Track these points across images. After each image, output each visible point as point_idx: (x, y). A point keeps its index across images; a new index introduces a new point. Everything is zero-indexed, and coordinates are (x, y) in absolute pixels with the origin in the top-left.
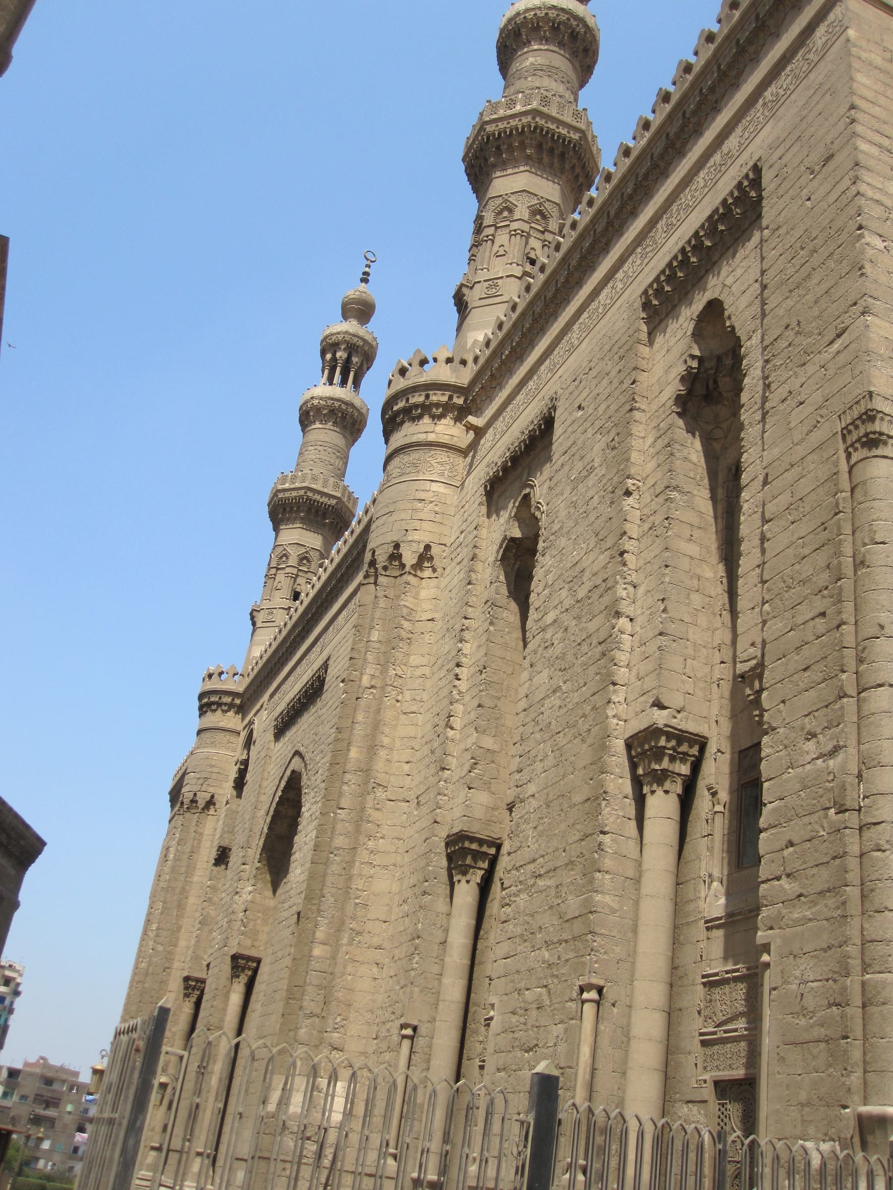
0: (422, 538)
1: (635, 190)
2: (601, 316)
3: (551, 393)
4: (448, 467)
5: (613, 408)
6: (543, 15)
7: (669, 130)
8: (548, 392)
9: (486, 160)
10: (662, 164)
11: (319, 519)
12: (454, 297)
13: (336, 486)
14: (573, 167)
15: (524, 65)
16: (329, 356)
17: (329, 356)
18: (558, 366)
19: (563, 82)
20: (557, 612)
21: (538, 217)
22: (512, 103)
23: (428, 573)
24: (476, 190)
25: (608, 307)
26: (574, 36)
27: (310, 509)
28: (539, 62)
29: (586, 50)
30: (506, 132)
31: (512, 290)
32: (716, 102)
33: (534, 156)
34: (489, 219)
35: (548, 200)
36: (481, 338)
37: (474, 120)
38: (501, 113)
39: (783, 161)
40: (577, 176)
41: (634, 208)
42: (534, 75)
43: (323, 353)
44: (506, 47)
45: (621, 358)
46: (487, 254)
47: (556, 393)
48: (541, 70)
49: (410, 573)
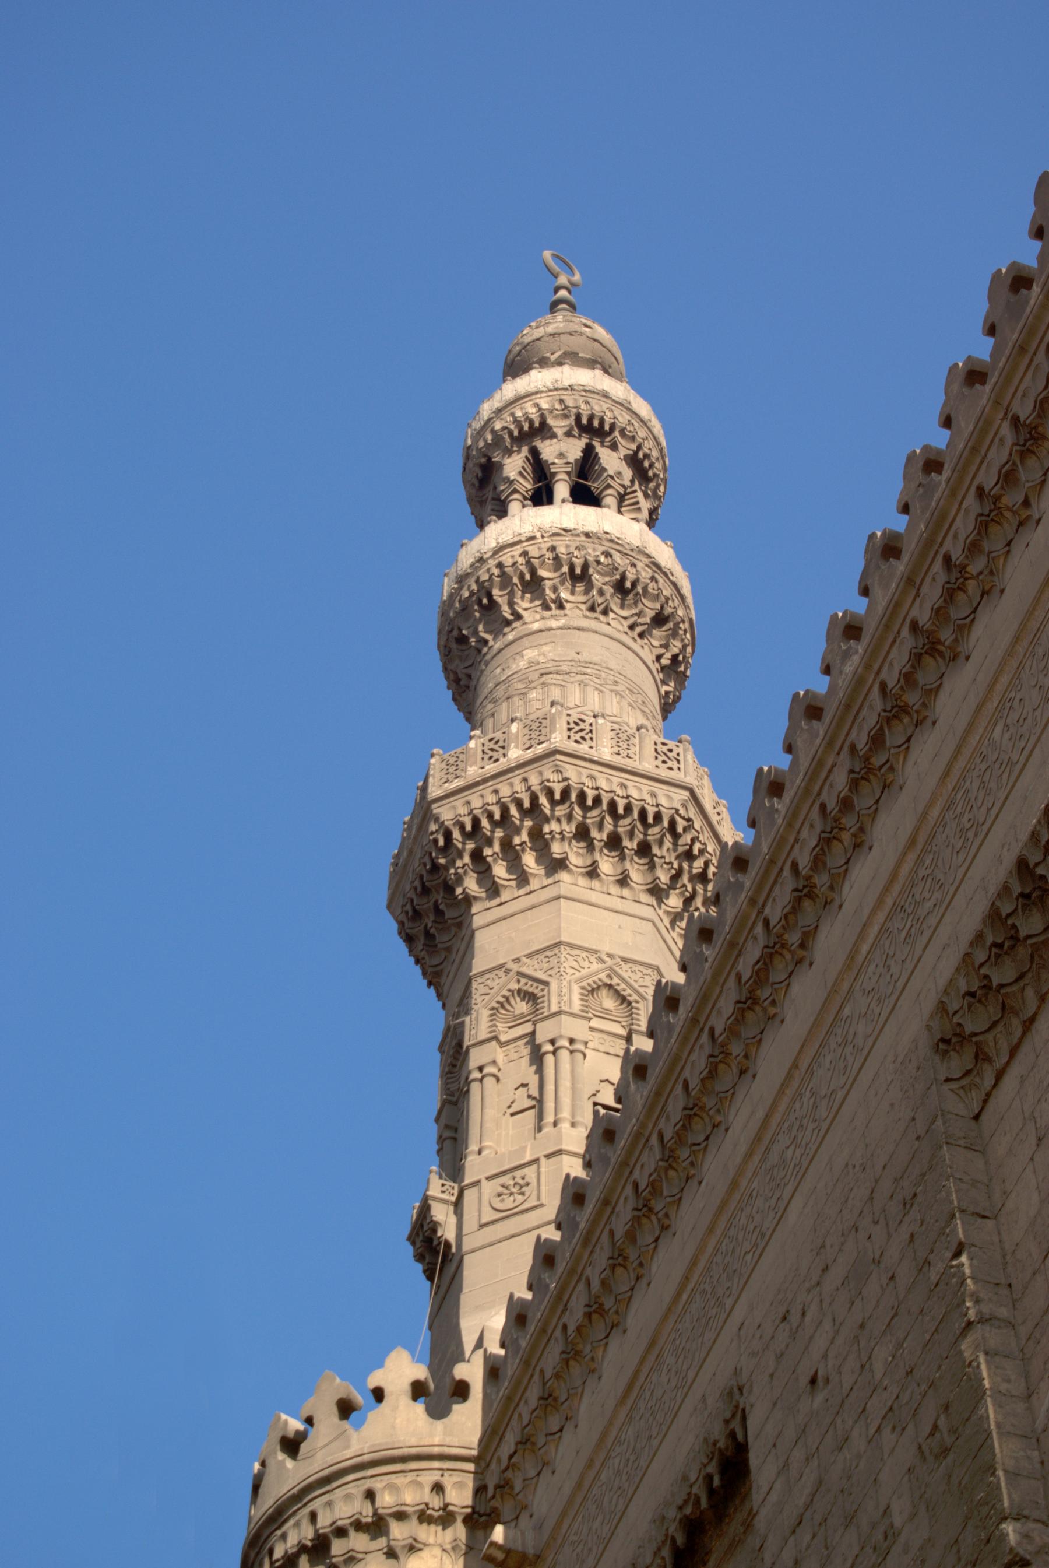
1: (854, 784)
2: (824, 1126)
7: (914, 613)
10: (912, 698)
12: (412, 1239)
15: (514, 668)
18: (729, 1302)
19: (617, 693)
21: (609, 1003)
24: (434, 978)
25: (840, 1095)
28: (551, 655)
32: (1026, 503)
35: (626, 960)
36: (497, 1320)
41: (862, 829)
45: (907, 1204)
47: (736, 1372)
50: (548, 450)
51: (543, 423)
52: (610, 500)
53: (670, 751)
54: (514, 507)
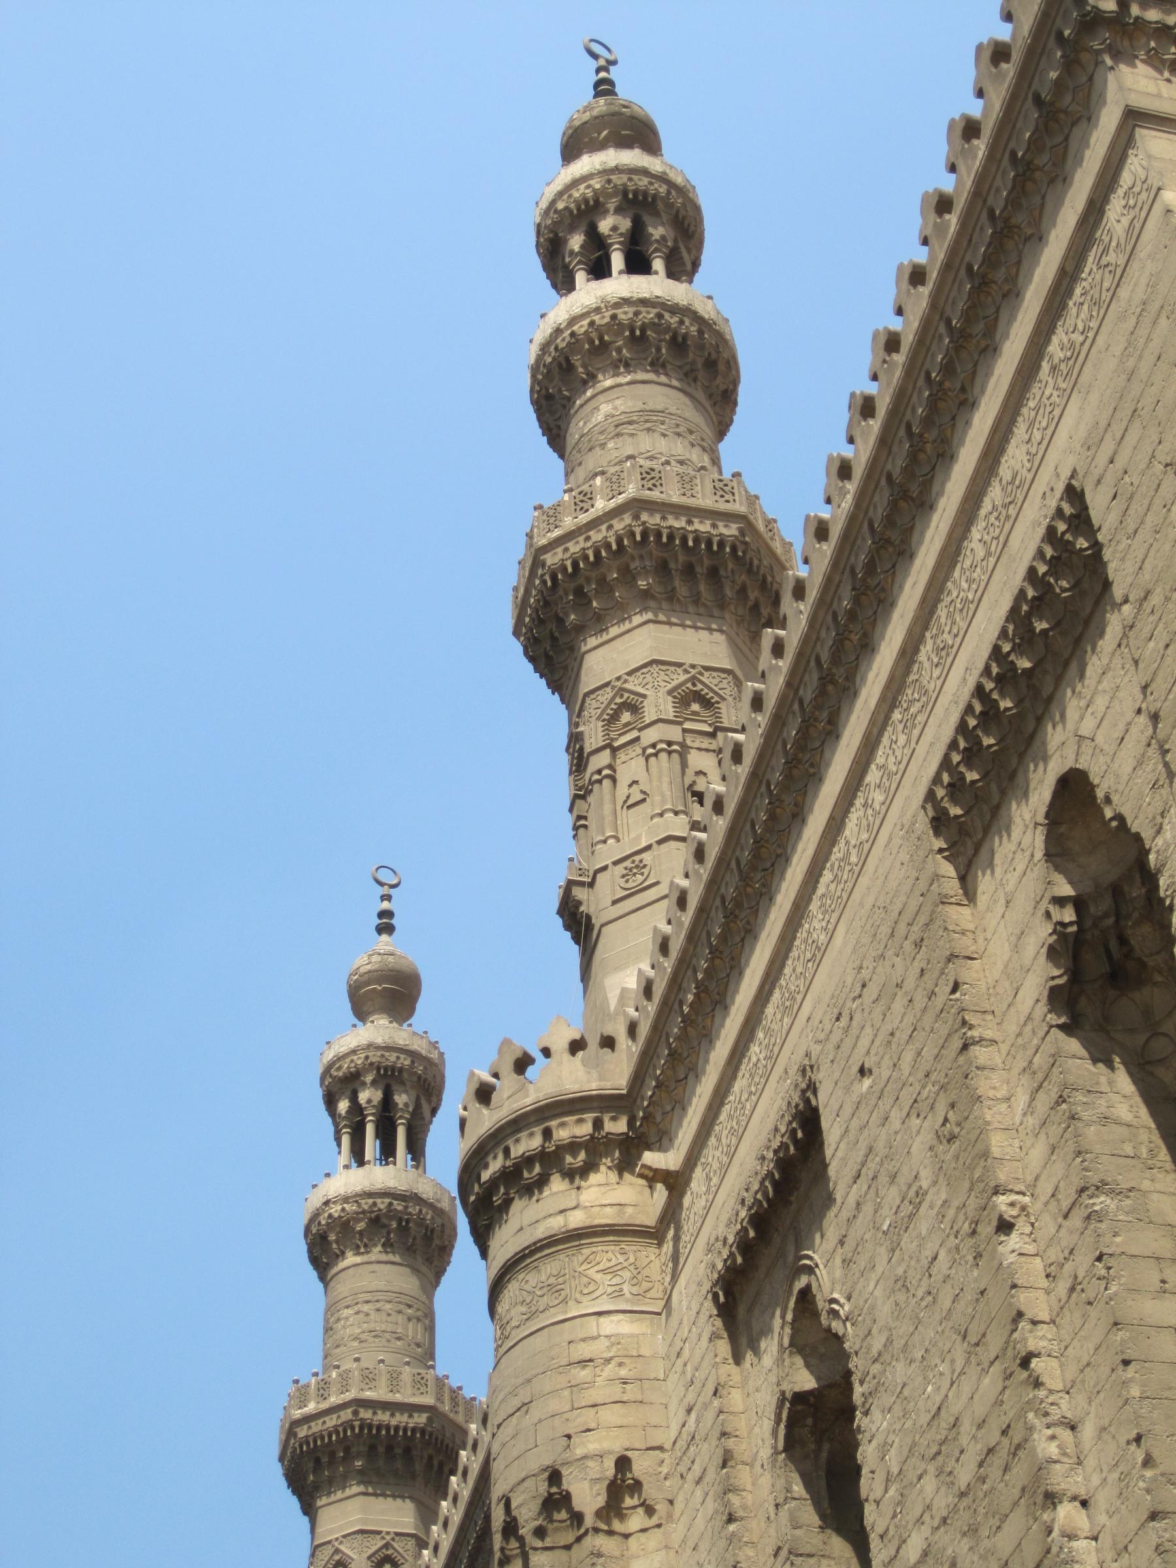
0: (606, 1445)
1: (856, 600)
2: (857, 869)
3: (798, 1058)
4: (627, 1275)
5: (929, 1053)
6: (607, 320)
7: (889, 467)
8: (791, 1057)
9: (560, 621)
10: (895, 536)
11: (399, 1464)
12: (560, 912)
13: (419, 1383)
14: (742, 591)
15: (594, 421)
16: (343, 1106)
17: (343, 1106)
18: (799, 998)
19: (678, 434)
20: (926, 1530)
21: (695, 707)
22: (584, 499)
23: (636, 1520)
24: (555, 686)
25: (867, 846)
26: (679, 344)
27: (372, 1448)
28: (622, 408)
29: (711, 365)
30: (586, 558)
31: (673, 869)
32: (963, 389)
33: (658, 589)
34: (594, 735)
35: (707, 669)
36: (632, 982)
37: (519, 551)
38: (569, 522)
39: (1120, 463)
40: (755, 608)
41: (865, 635)
42: (618, 435)
43: (330, 1101)
44: (549, 397)
45: (918, 945)
46: (607, 808)
47: (808, 1055)
48: (630, 423)
49: (596, 1530)
50: (605, 226)
51: (597, 201)
52: (658, 264)
53: (726, 485)
54: (580, 277)
